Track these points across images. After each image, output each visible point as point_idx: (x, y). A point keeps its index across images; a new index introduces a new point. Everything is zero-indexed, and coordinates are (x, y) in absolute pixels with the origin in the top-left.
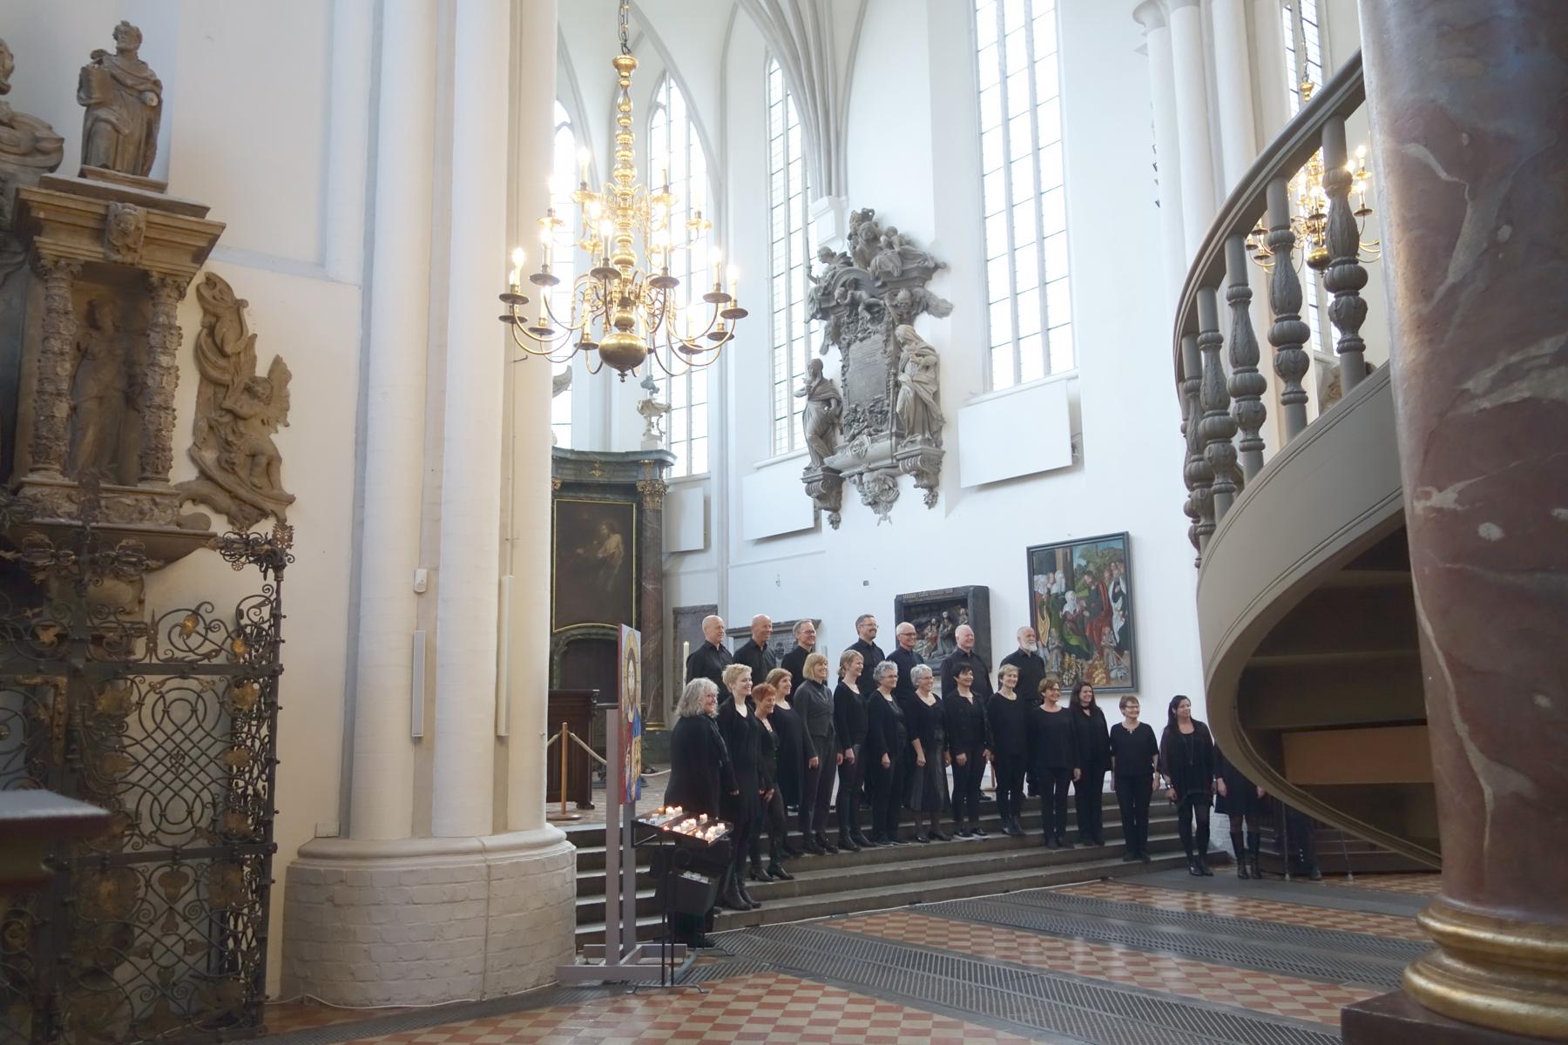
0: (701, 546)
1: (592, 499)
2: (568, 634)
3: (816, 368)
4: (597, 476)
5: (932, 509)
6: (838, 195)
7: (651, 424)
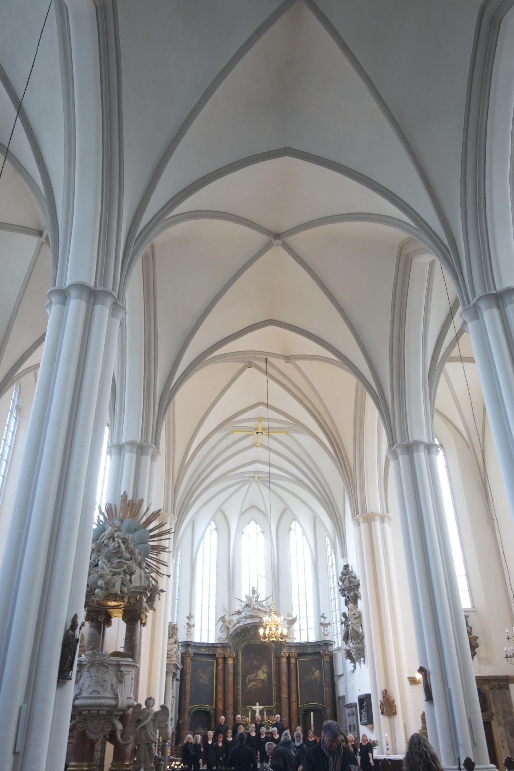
0: (342, 674)
1: (309, 658)
2: (303, 708)
3: (344, 615)
4: (310, 650)
5: (478, 636)
6: (346, 557)
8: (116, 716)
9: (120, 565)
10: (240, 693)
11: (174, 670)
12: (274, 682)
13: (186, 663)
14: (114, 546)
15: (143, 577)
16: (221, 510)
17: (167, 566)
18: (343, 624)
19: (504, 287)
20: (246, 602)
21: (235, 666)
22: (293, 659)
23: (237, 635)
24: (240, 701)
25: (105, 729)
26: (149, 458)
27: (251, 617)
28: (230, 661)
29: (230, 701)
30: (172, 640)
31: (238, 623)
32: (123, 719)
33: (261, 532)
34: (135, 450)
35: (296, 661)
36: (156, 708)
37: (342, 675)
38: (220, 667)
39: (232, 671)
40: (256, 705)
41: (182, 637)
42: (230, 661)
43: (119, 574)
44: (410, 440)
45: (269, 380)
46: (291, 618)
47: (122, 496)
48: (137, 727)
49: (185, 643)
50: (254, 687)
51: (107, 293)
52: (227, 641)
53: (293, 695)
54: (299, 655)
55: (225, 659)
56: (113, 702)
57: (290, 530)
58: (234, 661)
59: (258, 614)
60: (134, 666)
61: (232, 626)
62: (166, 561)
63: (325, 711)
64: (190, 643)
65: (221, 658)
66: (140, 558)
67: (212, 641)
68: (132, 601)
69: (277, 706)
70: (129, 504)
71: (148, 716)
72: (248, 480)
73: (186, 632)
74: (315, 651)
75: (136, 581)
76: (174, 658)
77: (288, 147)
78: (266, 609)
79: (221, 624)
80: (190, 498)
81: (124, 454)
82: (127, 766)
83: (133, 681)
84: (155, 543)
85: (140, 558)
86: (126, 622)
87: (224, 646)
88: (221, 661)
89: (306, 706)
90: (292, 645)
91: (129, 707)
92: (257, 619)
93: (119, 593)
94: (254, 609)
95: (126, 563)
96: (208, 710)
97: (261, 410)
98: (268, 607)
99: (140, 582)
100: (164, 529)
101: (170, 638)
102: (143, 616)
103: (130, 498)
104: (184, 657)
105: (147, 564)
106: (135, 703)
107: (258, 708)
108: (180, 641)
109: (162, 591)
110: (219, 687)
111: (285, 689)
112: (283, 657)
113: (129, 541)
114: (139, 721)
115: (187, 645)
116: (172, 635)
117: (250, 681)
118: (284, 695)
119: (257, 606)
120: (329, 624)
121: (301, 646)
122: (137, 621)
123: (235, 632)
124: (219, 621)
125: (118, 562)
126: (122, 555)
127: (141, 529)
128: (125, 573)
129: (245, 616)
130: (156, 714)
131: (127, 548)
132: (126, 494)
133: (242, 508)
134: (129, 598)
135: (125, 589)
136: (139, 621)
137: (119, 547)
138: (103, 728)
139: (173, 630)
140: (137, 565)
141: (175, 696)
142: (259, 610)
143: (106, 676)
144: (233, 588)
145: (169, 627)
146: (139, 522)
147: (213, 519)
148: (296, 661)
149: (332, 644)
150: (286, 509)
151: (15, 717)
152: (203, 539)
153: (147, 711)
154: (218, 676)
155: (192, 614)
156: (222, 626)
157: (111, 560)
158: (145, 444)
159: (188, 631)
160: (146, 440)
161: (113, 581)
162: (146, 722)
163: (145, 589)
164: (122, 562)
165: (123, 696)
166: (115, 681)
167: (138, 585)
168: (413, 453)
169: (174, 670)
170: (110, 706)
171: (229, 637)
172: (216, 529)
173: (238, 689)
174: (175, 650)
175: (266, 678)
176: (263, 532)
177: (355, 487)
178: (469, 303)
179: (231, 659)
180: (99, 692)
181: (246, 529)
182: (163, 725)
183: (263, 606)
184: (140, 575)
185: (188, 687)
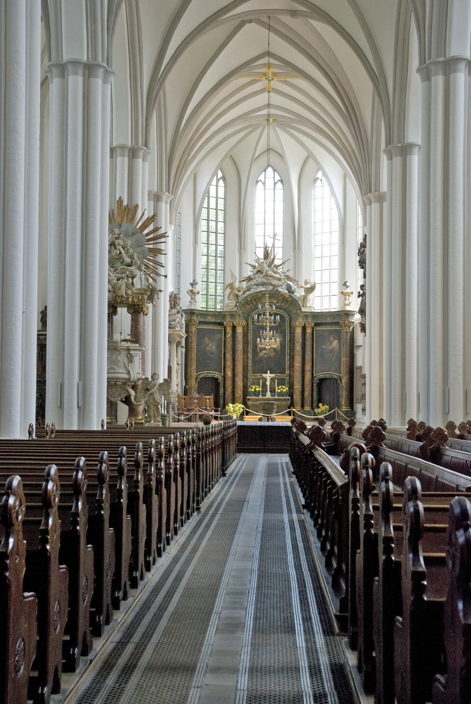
4: (329, 320)
7: (345, 299)
8: (129, 385)
10: (250, 361)
12: (287, 351)
13: (192, 331)
14: (116, 253)
15: (143, 279)
17: (163, 267)
18: (361, 298)
19: (452, 55)
20: (258, 267)
21: (245, 335)
22: (310, 328)
23: (247, 303)
24: (250, 368)
25: (122, 394)
26: (140, 161)
27: (263, 284)
28: (239, 330)
29: (239, 368)
32: (134, 387)
33: (279, 181)
34: (126, 153)
35: (313, 331)
37: (361, 346)
38: (229, 336)
39: (242, 340)
40: (267, 373)
41: (185, 303)
44: (405, 142)
45: (273, 36)
46: (309, 286)
47: (118, 201)
48: (146, 394)
49: (189, 311)
50: (266, 356)
51: (99, 66)
52: (235, 309)
53: (307, 364)
55: (234, 328)
56: (126, 376)
59: (271, 281)
61: (241, 293)
62: (163, 262)
63: (341, 381)
64: (195, 311)
66: (139, 262)
68: (136, 300)
69: (289, 375)
70: (125, 209)
71: (154, 386)
72: (260, 124)
73: (190, 300)
74: (334, 321)
75: (138, 284)
76: (177, 327)
78: (280, 276)
79: (228, 291)
80: (189, 155)
81: (116, 157)
82: (140, 420)
83: (140, 361)
84: (151, 246)
85: (139, 262)
86: (130, 313)
87: (232, 315)
88: (229, 330)
89: (321, 375)
90: (308, 314)
91: (139, 379)
92: (270, 286)
93: (124, 295)
94: (267, 275)
96: (216, 377)
98: (282, 273)
99: (141, 283)
100: (159, 232)
102: (145, 309)
103: (125, 203)
106: (144, 377)
107: (268, 376)
109: (161, 291)
110: (227, 355)
111: (298, 359)
113: (128, 247)
114: (147, 390)
115: (191, 313)
116: (174, 305)
117: (261, 351)
118: (298, 364)
119: (271, 273)
120: (352, 293)
122: (140, 313)
123: (245, 300)
124: (227, 288)
125: (121, 269)
127: (137, 233)
129: (256, 283)
130: (160, 385)
131: (127, 253)
132: (122, 199)
134: (133, 298)
135: (129, 292)
136: (142, 313)
137: (120, 253)
138: (120, 393)
140: (137, 268)
141: (180, 363)
142: (272, 277)
143: (119, 358)
144: (244, 249)
145: (170, 297)
146: (135, 227)
148: (313, 331)
149: (354, 314)
150: (310, 156)
151: (76, 389)
153: (153, 382)
154: (227, 344)
156: (231, 293)
157: (114, 265)
158: (136, 146)
159: (191, 298)
162: (153, 390)
163: (146, 290)
164: (125, 268)
165: (133, 372)
166: (126, 361)
167: (139, 287)
169: (178, 339)
170: (124, 379)
171: (238, 304)
172: (224, 178)
173: (248, 357)
174: (178, 320)
175: (279, 347)
176: (281, 181)
177: (369, 161)
178: (425, 63)
179: (240, 327)
181: (262, 177)
182: (166, 393)
184: (141, 277)
185: (194, 355)
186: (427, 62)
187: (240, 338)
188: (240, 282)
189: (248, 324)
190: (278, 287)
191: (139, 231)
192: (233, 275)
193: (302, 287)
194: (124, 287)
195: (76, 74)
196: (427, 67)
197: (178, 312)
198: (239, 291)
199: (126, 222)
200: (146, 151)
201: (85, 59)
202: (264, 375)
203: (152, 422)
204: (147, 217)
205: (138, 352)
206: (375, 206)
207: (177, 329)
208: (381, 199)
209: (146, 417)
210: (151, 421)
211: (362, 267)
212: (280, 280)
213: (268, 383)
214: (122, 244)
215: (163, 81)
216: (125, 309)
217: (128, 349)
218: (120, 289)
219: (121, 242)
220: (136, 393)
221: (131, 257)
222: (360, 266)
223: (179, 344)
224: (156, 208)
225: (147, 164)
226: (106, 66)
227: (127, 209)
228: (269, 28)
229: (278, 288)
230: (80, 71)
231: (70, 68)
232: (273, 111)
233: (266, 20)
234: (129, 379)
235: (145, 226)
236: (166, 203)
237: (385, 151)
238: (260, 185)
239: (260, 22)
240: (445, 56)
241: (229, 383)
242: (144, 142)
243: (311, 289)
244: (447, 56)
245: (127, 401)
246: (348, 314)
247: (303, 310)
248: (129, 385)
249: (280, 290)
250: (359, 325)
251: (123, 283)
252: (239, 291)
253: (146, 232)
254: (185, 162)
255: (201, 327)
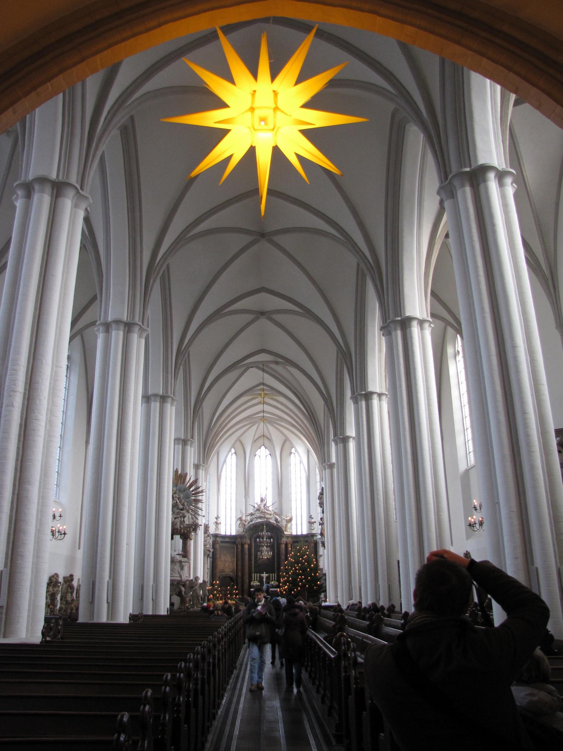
7: (311, 526)
8: (181, 584)
9: (178, 513)
11: (208, 553)
13: (216, 547)
15: (190, 518)
16: (239, 440)
19: (369, 390)
21: (250, 549)
22: (290, 545)
27: (260, 517)
28: (246, 546)
30: (207, 535)
31: (251, 521)
32: (184, 586)
34: (181, 443)
36: (201, 581)
37: (322, 555)
38: (239, 550)
40: (263, 573)
41: (212, 531)
42: (246, 546)
43: (178, 518)
46: (288, 518)
48: (191, 590)
50: (262, 563)
51: (169, 397)
52: (243, 533)
54: (294, 542)
55: (243, 545)
56: (179, 579)
57: (291, 453)
58: (248, 546)
60: (188, 562)
61: (247, 523)
64: (218, 535)
65: (240, 544)
66: (188, 508)
67: (234, 533)
68: (186, 532)
70: (179, 476)
71: (197, 585)
73: (215, 528)
75: (187, 521)
77: (264, 287)
78: (271, 512)
79: (239, 522)
80: (215, 441)
85: (188, 508)
88: (239, 546)
90: (288, 536)
91: (187, 581)
94: (262, 512)
95: (181, 512)
97: (262, 387)
100: (200, 489)
101: (204, 533)
103: (180, 472)
104: (214, 543)
105: (191, 509)
107: (265, 575)
108: (211, 533)
109: (201, 525)
112: (283, 544)
114: (192, 587)
115: (216, 536)
116: (206, 531)
121: (297, 537)
122: (187, 539)
126: (178, 507)
128: (181, 517)
130: (201, 584)
131: (181, 502)
133: (254, 436)
135: (182, 526)
137: (177, 502)
139: (207, 528)
142: (266, 513)
144: (248, 495)
147: (233, 446)
152: (226, 462)
155: (219, 516)
156: (240, 523)
159: (216, 527)
160: (187, 437)
161: (175, 522)
162: (196, 587)
163: (192, 525)
164: (179, 512)
166: (179, 570)
168: (346, 443)
170: (178, 580)
172: (235, 453)
176: (270, 455)
177: (324, 444)
178: (354, 394)
180: (172, 574)
181: (258, 452)
183: (269, 510)
186: (356, 394)
187: (247, 552)
188: (246, 516)
189: (251, 542)
190: (269, 519)
191: (188, 489)
192: (241, 512)
193: (284, 519)
194: (178, 523)
195: (156, 401)
196: (356, 396)
197: (208, 536)
198: (246, 522)
199: (180, 483)
200: (192, 441)
201: (162, 393)
202: (262, 575)
203: (195, 607)
204: (192, 481)
205: (187, 564)
206: (328, 471)
207: (207, 546)
208: (331, 466)
209: (191, 605)
210: (194, 607)
211: (321, 507)
212: (271, 515)
213: (264, 580)
214: (178, 496)
215: (203, 401)
216: (179, 536)
217: (181, 562)
218: (176, 524)
219: (177, 495)
220: (185, 589)
221: (183, 505)
222: (320, 506)
223: (209, 555)
224: (196, 474)
225: (193, 449)
226: (173, 397)
227: (181, 475)
228: (263, 370)
229: (270, 520)
230: (158, 399)
231: (152, 398)
232: (265, 415)
233: (261, 366)
234: (181, 580)
235: (191, 486)
236: (202, 470)
237: (333, 440)
238: (257, 457)
239: (258, 368)
240: (365, 391)
241: (240, 580)
242: (191, 436)
243: (290, 520)
244: (366, 391)
245: (179, 594)
246: (313, 535)
247: (286, 533)
248: (181, 584)
249: (271, 521)
250: (320, 542)
251: (178, 520)
252: (246, 522)
253: (191, 489)
254: (213, 444)
255: (222, 544)
